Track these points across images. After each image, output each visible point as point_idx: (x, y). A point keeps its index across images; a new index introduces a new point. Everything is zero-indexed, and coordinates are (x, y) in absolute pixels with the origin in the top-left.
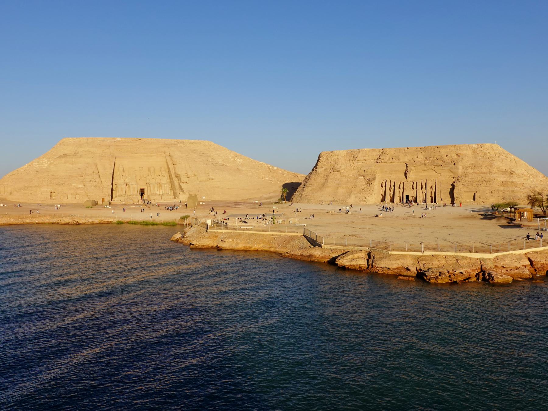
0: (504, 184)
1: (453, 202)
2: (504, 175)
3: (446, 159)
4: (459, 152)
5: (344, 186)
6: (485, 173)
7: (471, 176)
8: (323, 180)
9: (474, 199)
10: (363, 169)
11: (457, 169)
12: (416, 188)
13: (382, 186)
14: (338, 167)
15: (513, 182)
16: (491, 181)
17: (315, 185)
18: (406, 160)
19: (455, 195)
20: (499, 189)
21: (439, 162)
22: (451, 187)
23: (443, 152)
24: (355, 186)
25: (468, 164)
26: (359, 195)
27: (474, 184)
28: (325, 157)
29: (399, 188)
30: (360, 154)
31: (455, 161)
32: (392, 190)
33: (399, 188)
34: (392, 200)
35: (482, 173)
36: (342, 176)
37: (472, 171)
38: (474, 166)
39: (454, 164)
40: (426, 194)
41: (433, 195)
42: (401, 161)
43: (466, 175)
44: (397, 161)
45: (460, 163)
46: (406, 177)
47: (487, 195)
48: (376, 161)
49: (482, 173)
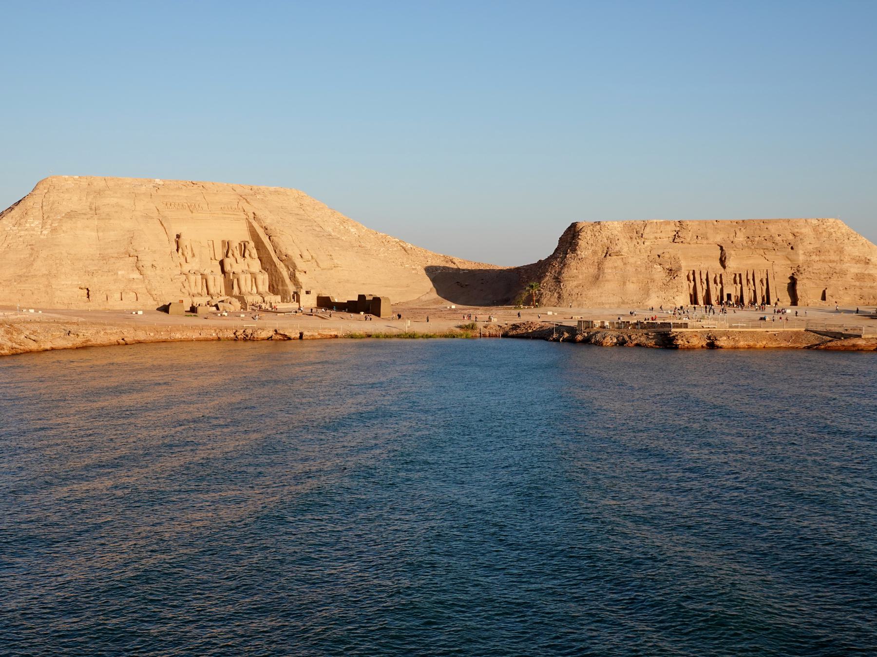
0: (860, 277)
1: (794, 302)
2: (858, 265)
3: (778, 239)
4: (796, 230)
5: (634, 279)
6: (834, 261)
7: (816, 266)
8: (593, 270)
9: (824, 298)
10: (656, 253)
11: (797, 254)
12: (741, 283)
13: (689, 279)
14: (617, 248)
15: (869, 275)
16: (843, 273)
17: (580, 277)
18: (719, 239)
19: (798, 292)
20: (855, 284)
21: (769, 244)
22: (789, 281)
23: (773, 229)
24: (653, 280)
25: (810, 247)
26: (662, 294)
27: (822, 277)
28: (589, 232)
29: (715, 282)
30: (648, 229)
31: (792, 243)
32: (705, 286)
33: (715, 282)
34: (707, 301)
35: (830, 261)
36: (625, 264)
37: (817, 258)
38: (819, 252)
39: (792, 248)
40: (755, 291)
41: (764, 293)
42: (711, 241)
43: (809, 264)
44: (705, 242)
45: (800, 247)
46: (724, 267)
47: (841, 292)
48: (671, 240)
49: (830, 261)
